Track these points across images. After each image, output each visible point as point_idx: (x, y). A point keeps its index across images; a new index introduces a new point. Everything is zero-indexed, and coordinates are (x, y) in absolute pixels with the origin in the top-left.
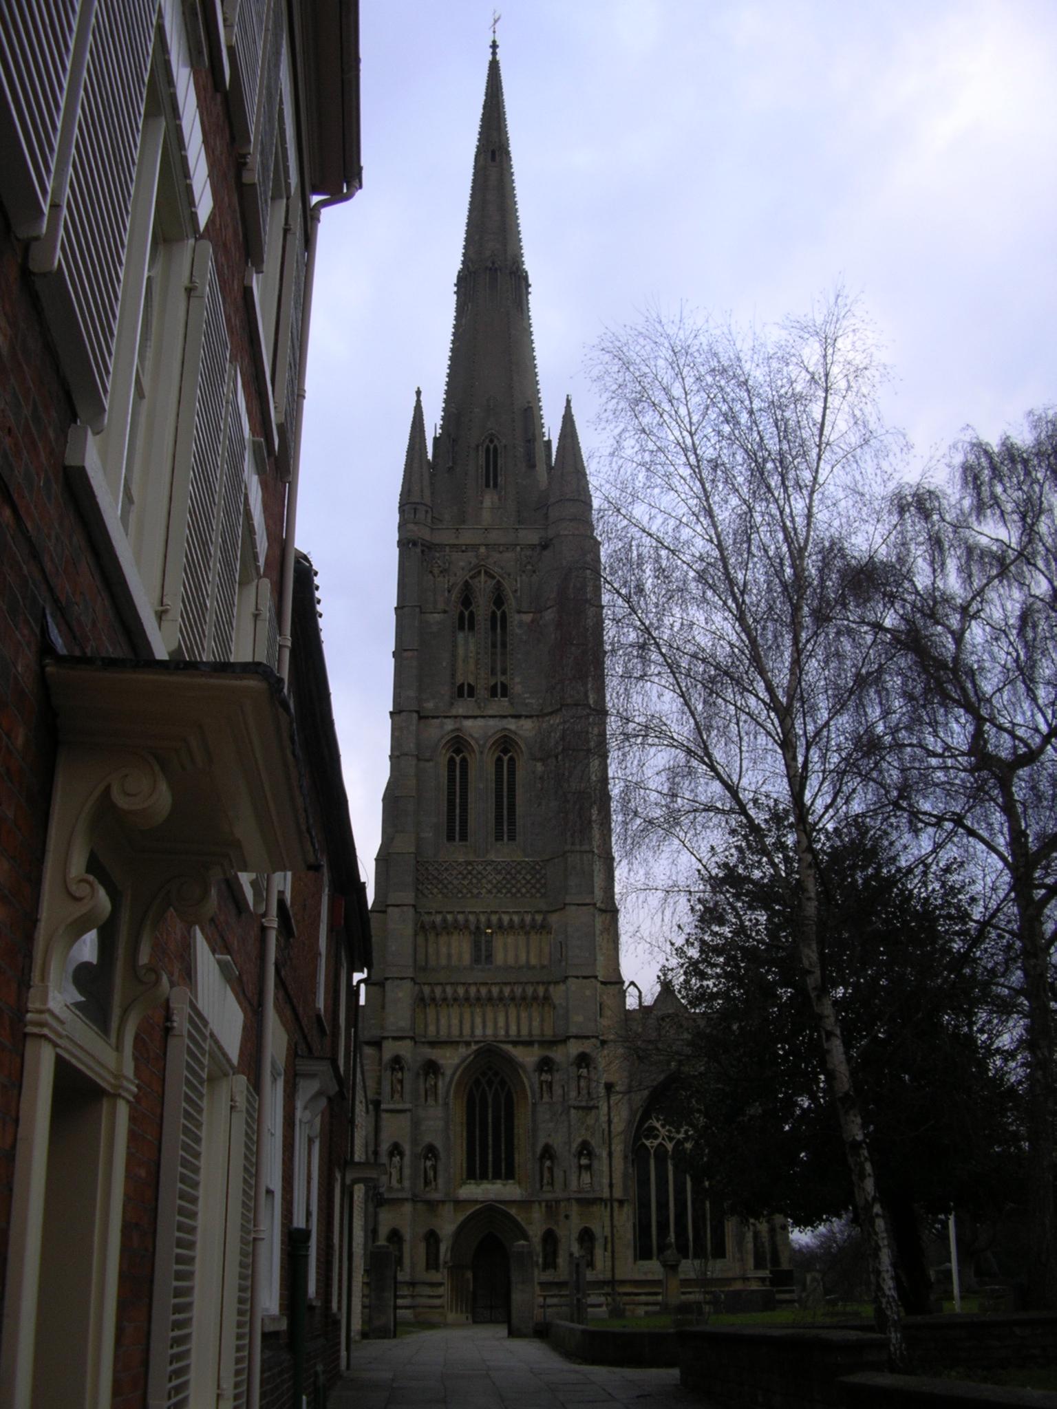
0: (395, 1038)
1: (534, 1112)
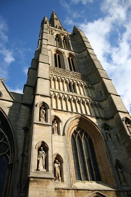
0: (42, 96)
1: (107, 145)
